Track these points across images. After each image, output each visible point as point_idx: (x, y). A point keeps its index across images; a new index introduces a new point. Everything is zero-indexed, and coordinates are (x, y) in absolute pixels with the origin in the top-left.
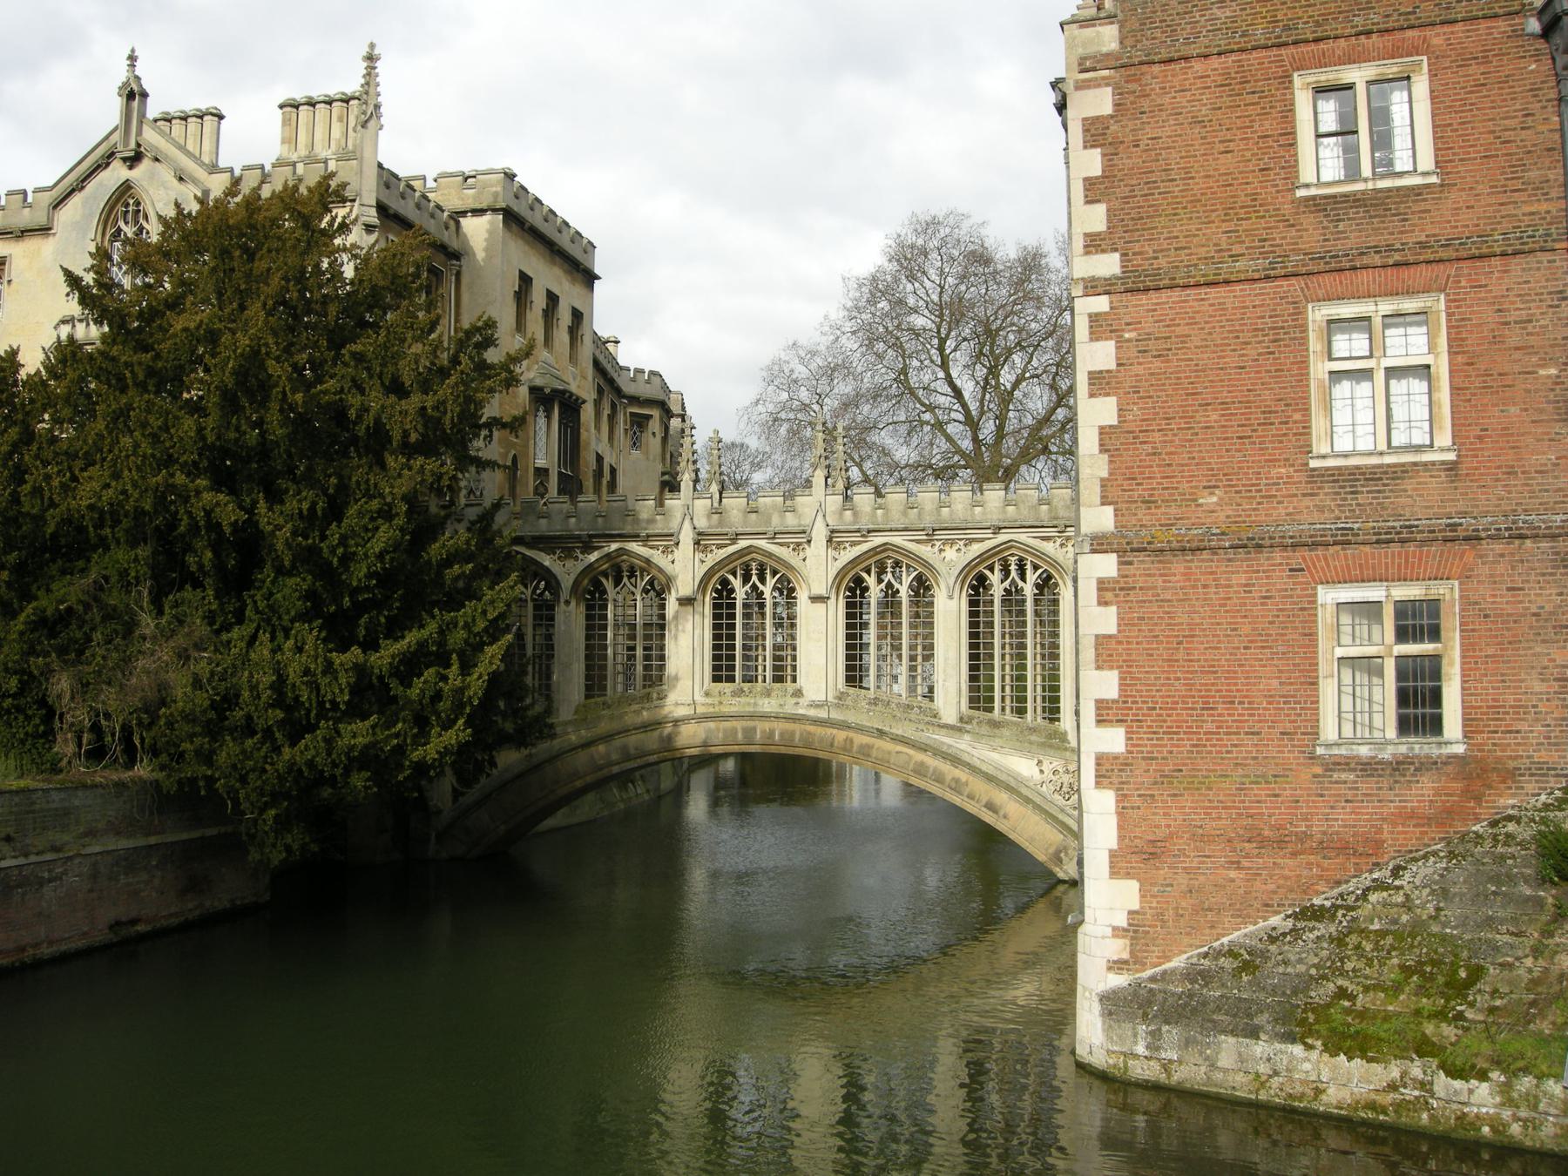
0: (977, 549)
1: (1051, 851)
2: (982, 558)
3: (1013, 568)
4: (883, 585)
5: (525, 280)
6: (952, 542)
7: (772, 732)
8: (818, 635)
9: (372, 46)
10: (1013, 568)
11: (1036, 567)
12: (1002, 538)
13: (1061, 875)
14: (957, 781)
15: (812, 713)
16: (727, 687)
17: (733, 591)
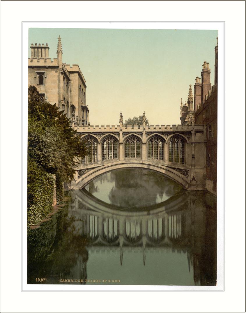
5: (80, 86)
9: (59, 36)
16: (127, 158)
17: (129, 142)
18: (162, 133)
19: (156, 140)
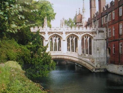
0: (83, 35)
1: (92, 69)
2: (83, 36)
3: (86, 37)
4: (71, 39)
6: (80, 34)
7: (59, 57)
8: (64, 44)
10: (86, 37)
11: (89, 37)
12: (86, 33)
13: (92, 71)
14: (81, 62)
15: (64, 55)
18: (77, 33)
19: (72, 38)
